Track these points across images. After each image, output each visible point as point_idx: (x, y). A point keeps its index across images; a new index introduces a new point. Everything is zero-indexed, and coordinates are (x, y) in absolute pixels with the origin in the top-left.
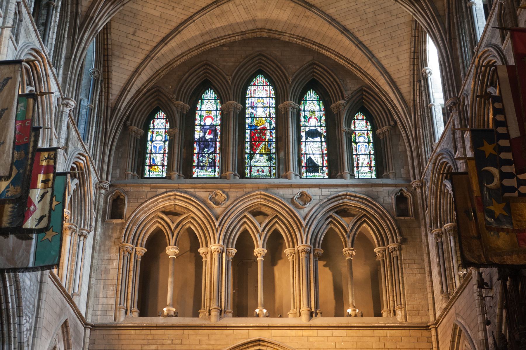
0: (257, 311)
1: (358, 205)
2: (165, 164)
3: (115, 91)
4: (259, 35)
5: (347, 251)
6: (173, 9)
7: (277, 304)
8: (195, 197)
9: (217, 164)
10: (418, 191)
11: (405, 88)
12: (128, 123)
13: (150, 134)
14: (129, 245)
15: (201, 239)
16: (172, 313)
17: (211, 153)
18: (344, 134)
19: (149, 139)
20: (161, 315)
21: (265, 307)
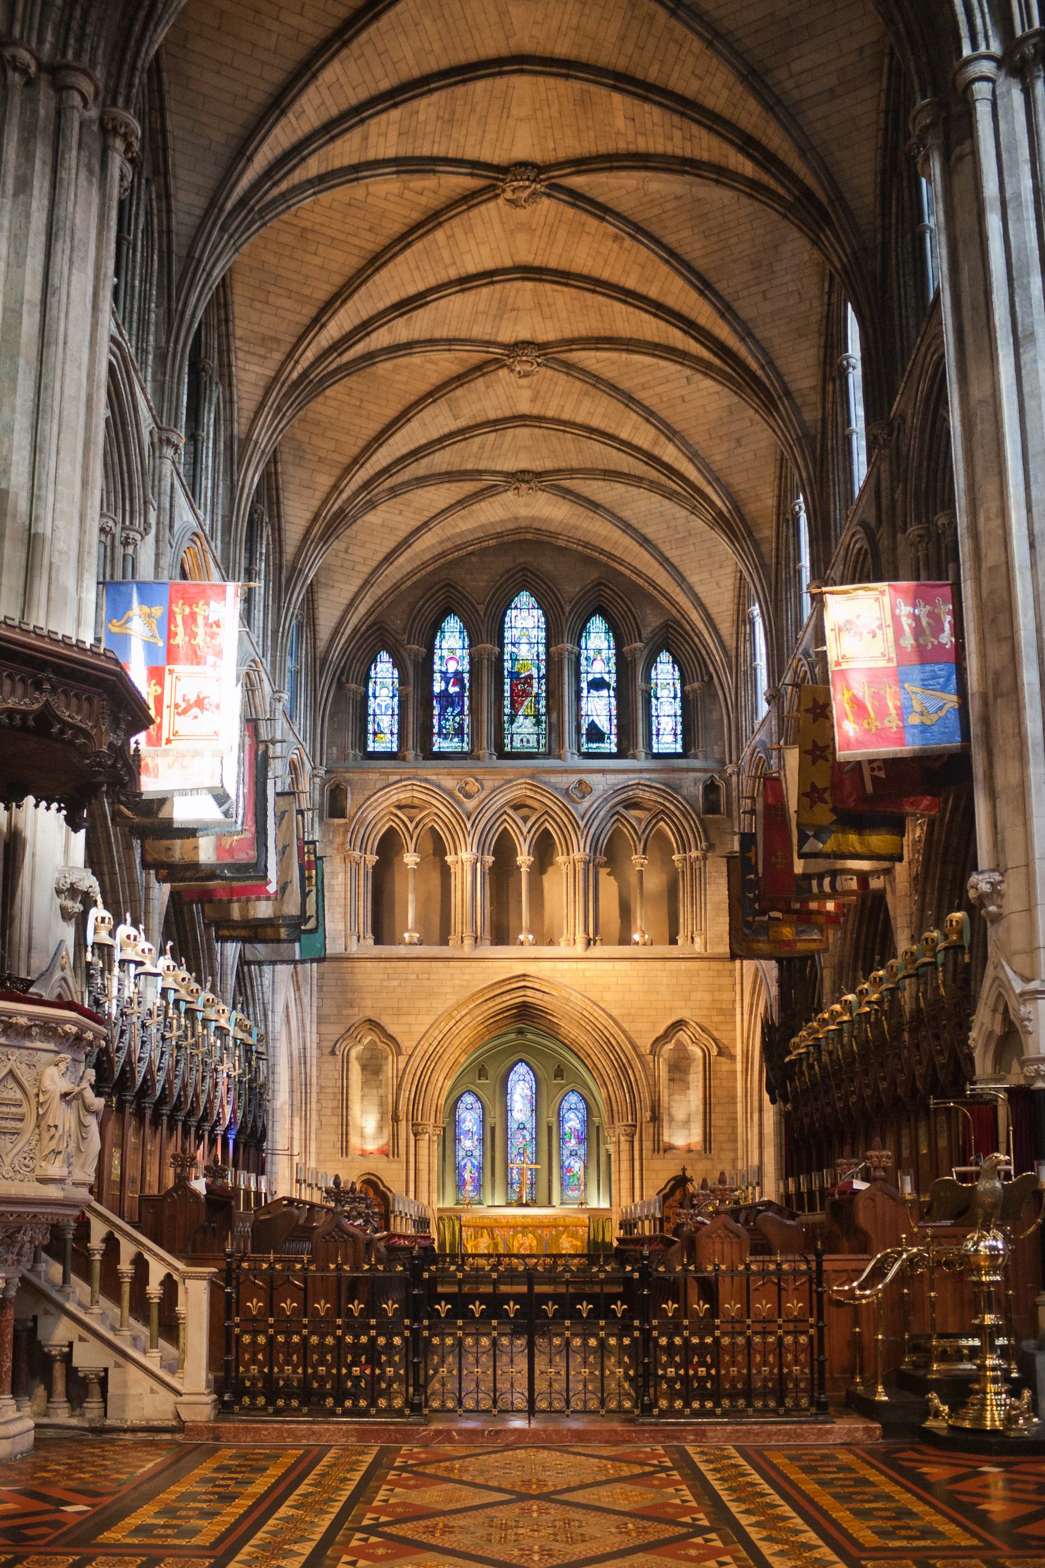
0: (522, 937)
1: (654, 797)
2: (395, 731)
3: (324, 633)
4: (522, 537)
6: (401, 512)
7: (546, 927)
8: (439, 787)
9: (466, 730)
10: (734, 778)
11: (726, 628)
12: (344, 679)
13: (371, 685)
14: (357, 853)
15: (449, 844)
17: (458, 714)
18: (639, 693)
19: (370, 693)
20: (402, 942)
21: (531, 931)
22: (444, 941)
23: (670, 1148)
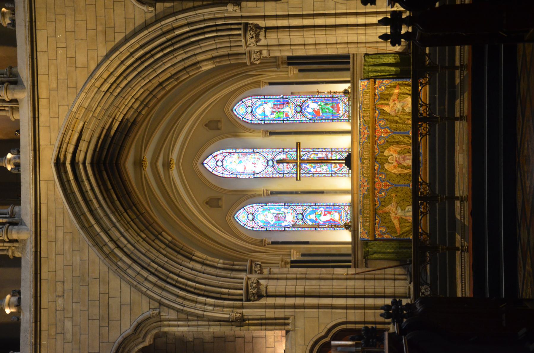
0: (9, 168)
16: (15, 299)
20: (16, 316)
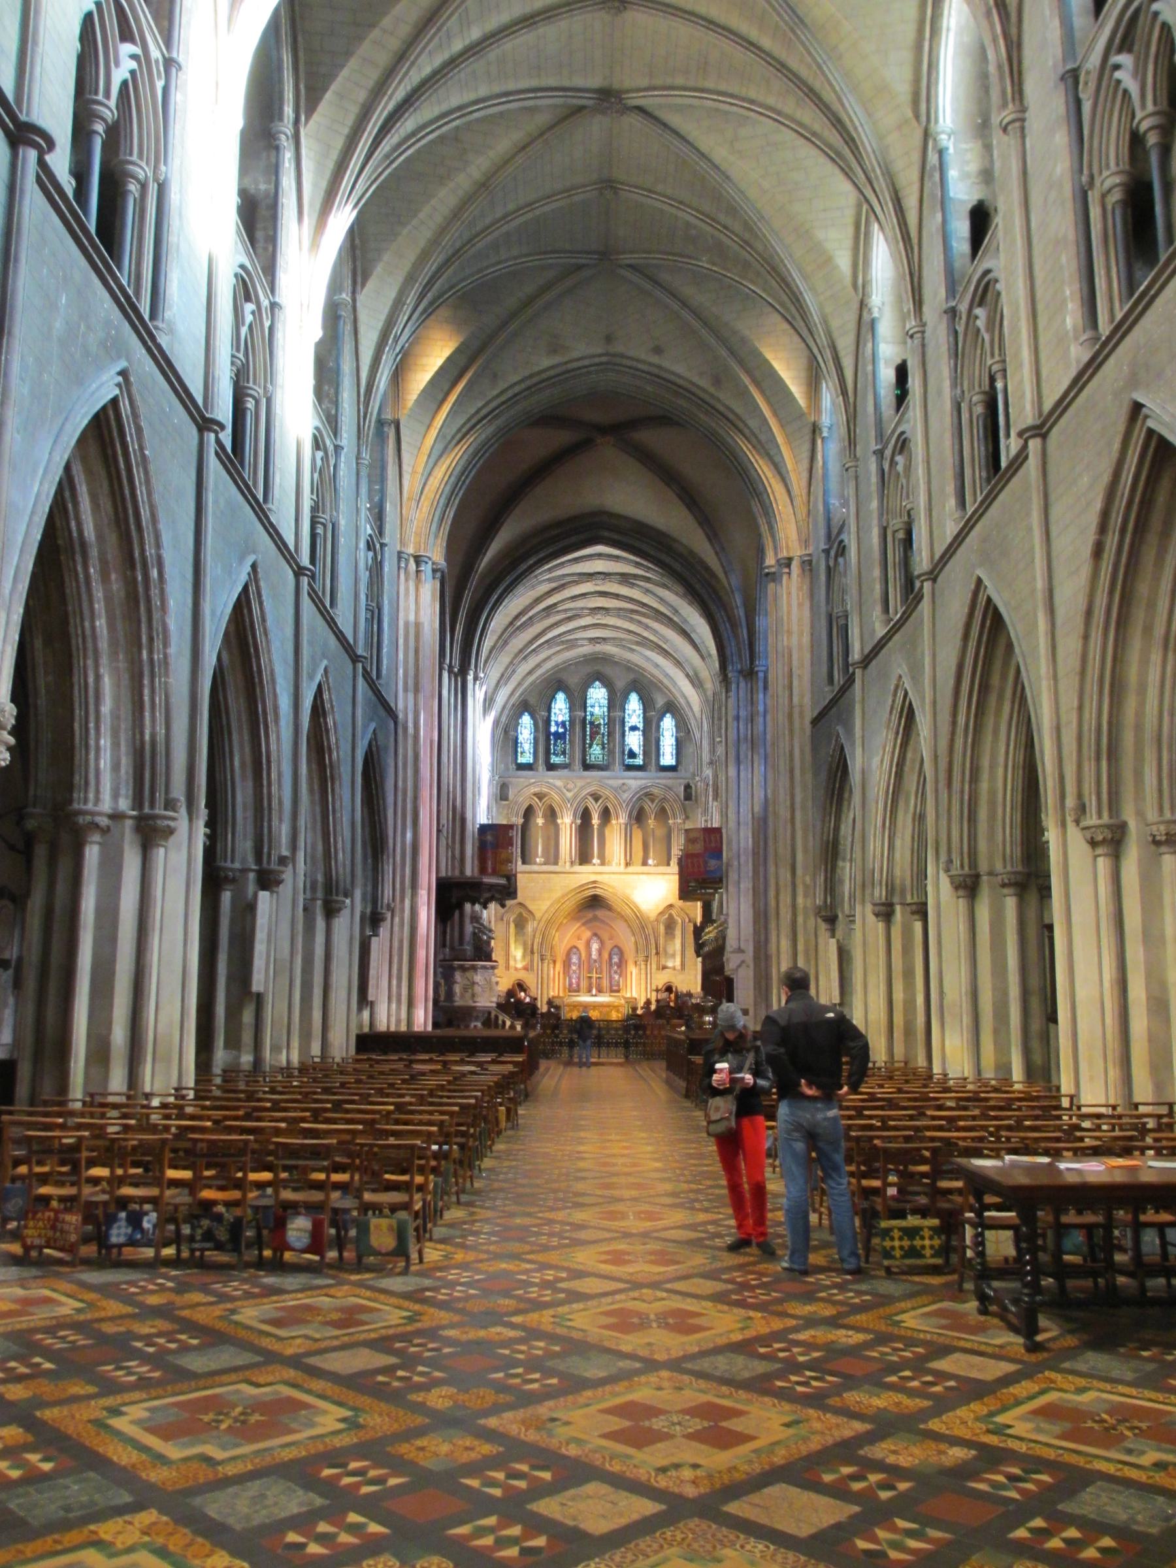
5: (651, 822)
15: (559, 814)
20: (535, 863)
21: (599, 857)
22: (556, 863)
23: (664, 968)
